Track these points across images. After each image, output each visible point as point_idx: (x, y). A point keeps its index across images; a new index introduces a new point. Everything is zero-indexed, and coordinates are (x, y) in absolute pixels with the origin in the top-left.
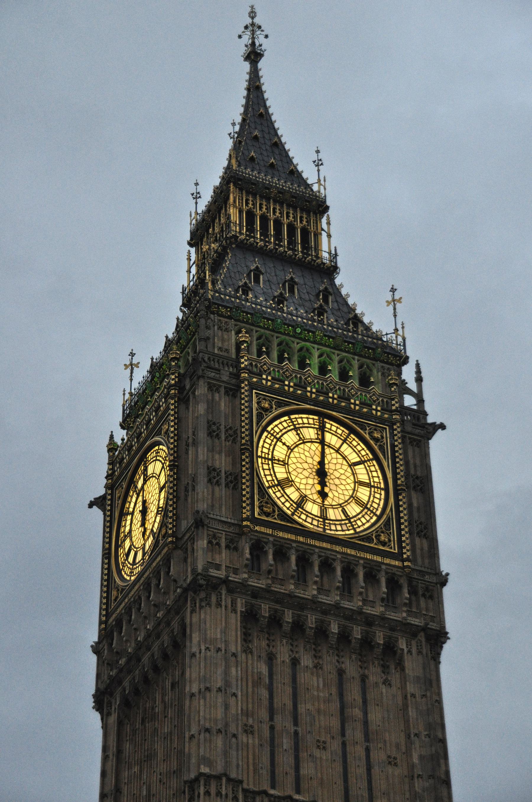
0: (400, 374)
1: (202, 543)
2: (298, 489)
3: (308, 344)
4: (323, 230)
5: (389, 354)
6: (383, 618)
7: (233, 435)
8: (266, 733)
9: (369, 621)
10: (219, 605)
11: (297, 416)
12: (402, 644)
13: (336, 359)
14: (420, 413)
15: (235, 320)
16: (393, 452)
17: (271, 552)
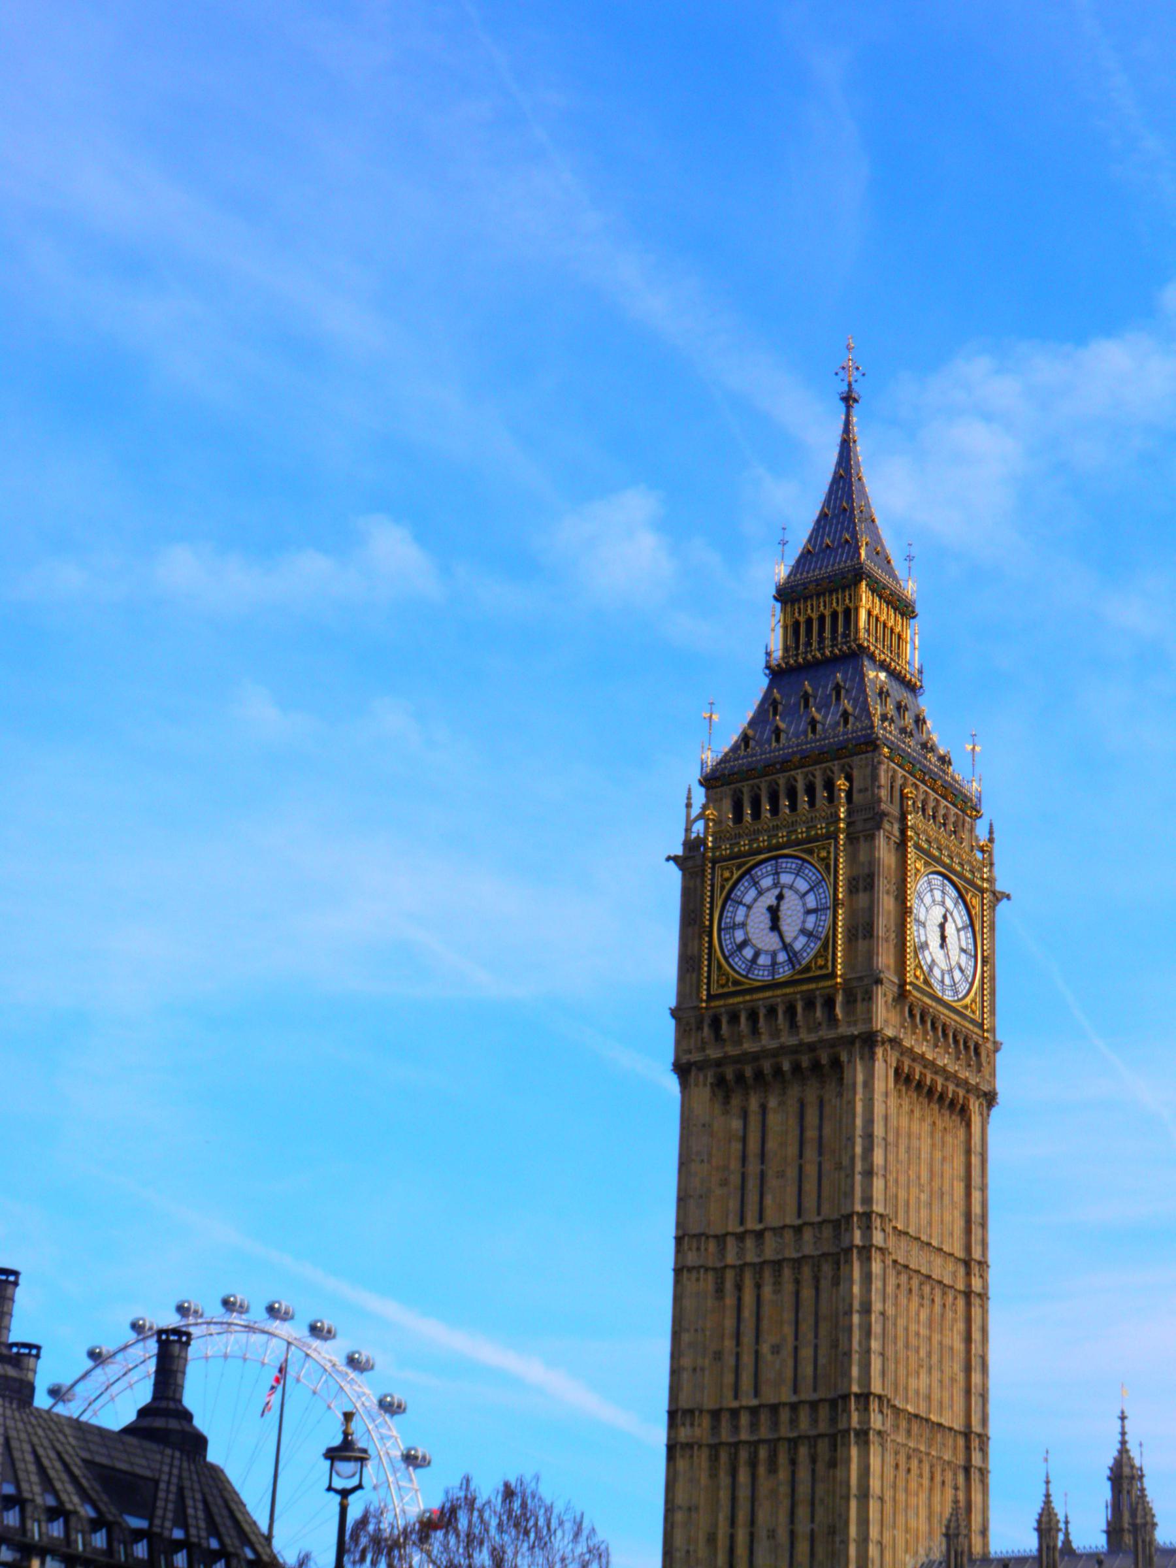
3: (792, 773)
6: (821, 1041)
8: (735, 1179)
9: (812, 1048)
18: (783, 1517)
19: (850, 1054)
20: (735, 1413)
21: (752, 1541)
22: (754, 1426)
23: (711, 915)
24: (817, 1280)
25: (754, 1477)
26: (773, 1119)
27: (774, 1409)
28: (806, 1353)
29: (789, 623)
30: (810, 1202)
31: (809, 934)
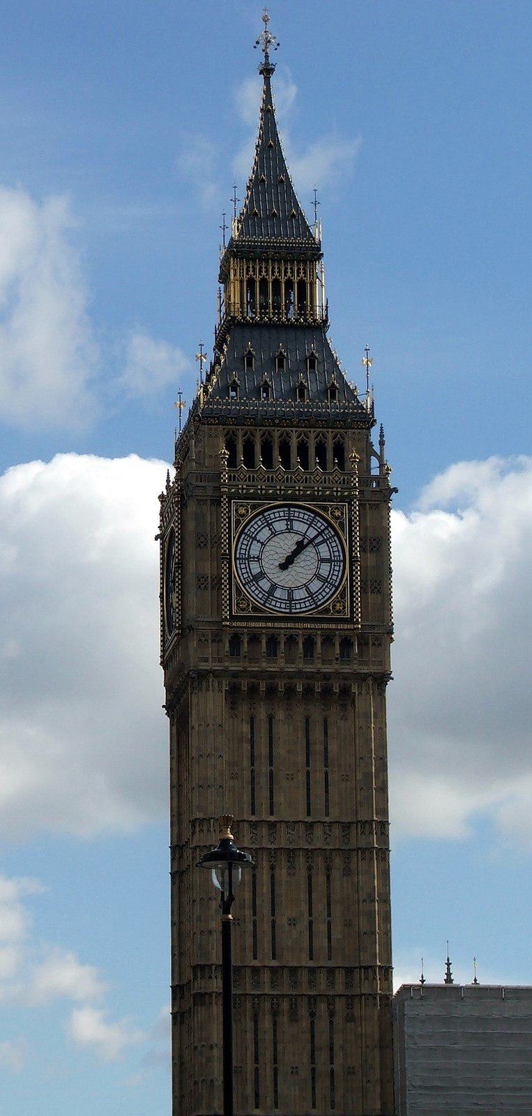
0: (368, 435)
1: (193, 644)
2: (269, 580)
3: (287, 429)
4: (318, 278)
5: (357, 421)
7: (217, 541)
9: (326, 677)
10: (208, 690)
11: (270, 512)
12: (355, 689)
13: (312, 436)
14: (383, 478)
15: (223, 425)
16: (351, 526)
17: (246, 640)
18: (306, 1059)
19: (360, 687)
20: (255, 970)
21: (276, 1075)
22: (273, 984)
23: (230, 544)
24: (328, 869)
25: (275, 1024)
26: (282, 730)
27: (294, 970)
28: (321, 927)
29: (245, 279)
30: (318, 803)
31: (325, 580)
